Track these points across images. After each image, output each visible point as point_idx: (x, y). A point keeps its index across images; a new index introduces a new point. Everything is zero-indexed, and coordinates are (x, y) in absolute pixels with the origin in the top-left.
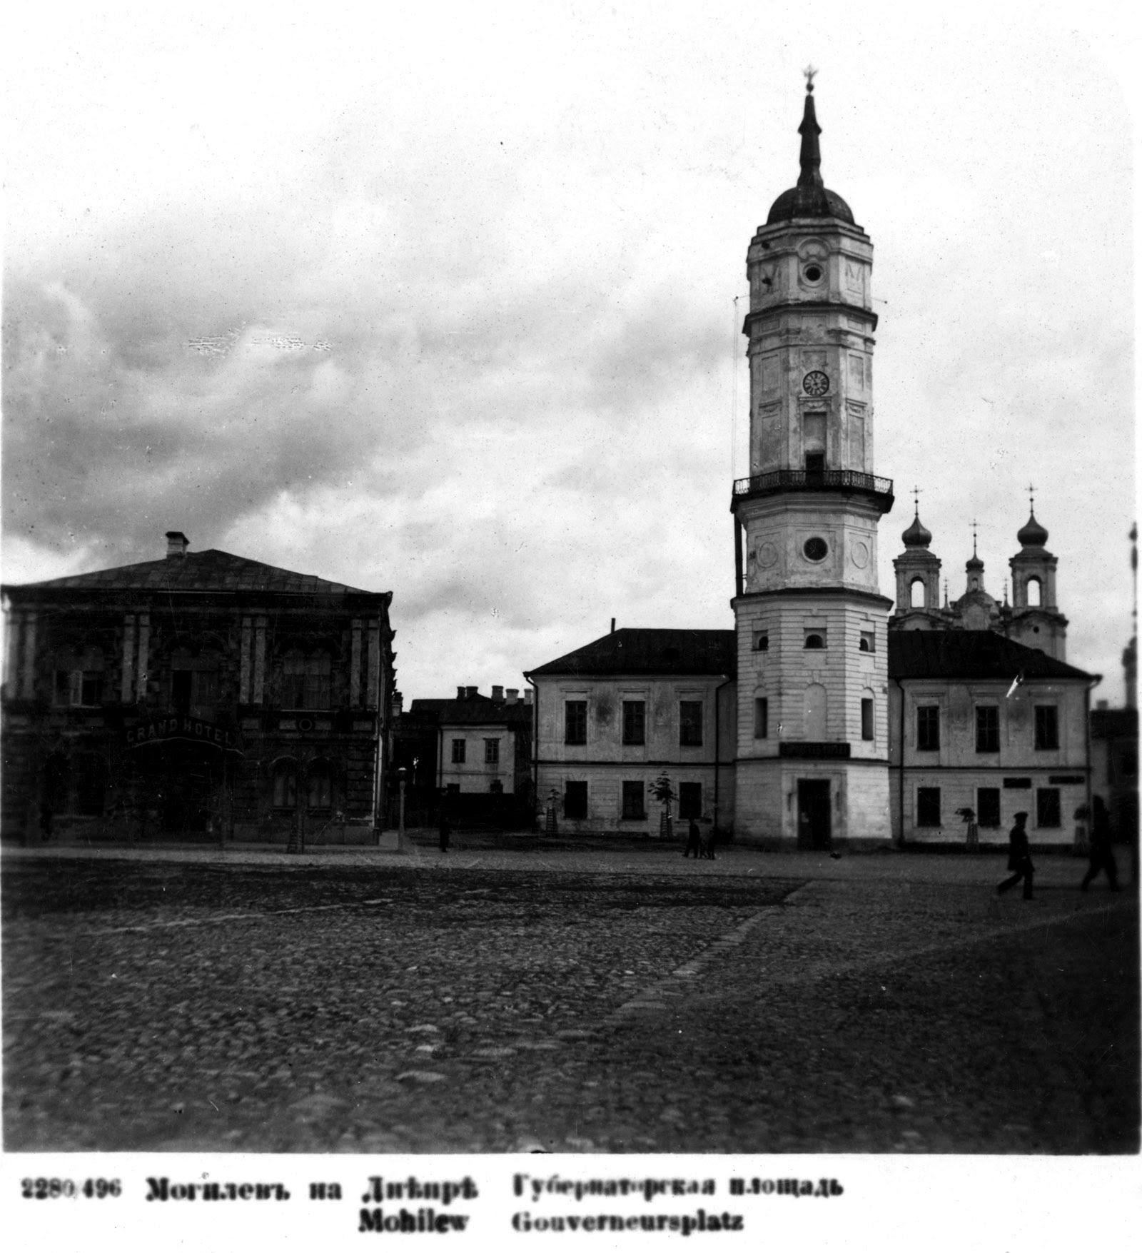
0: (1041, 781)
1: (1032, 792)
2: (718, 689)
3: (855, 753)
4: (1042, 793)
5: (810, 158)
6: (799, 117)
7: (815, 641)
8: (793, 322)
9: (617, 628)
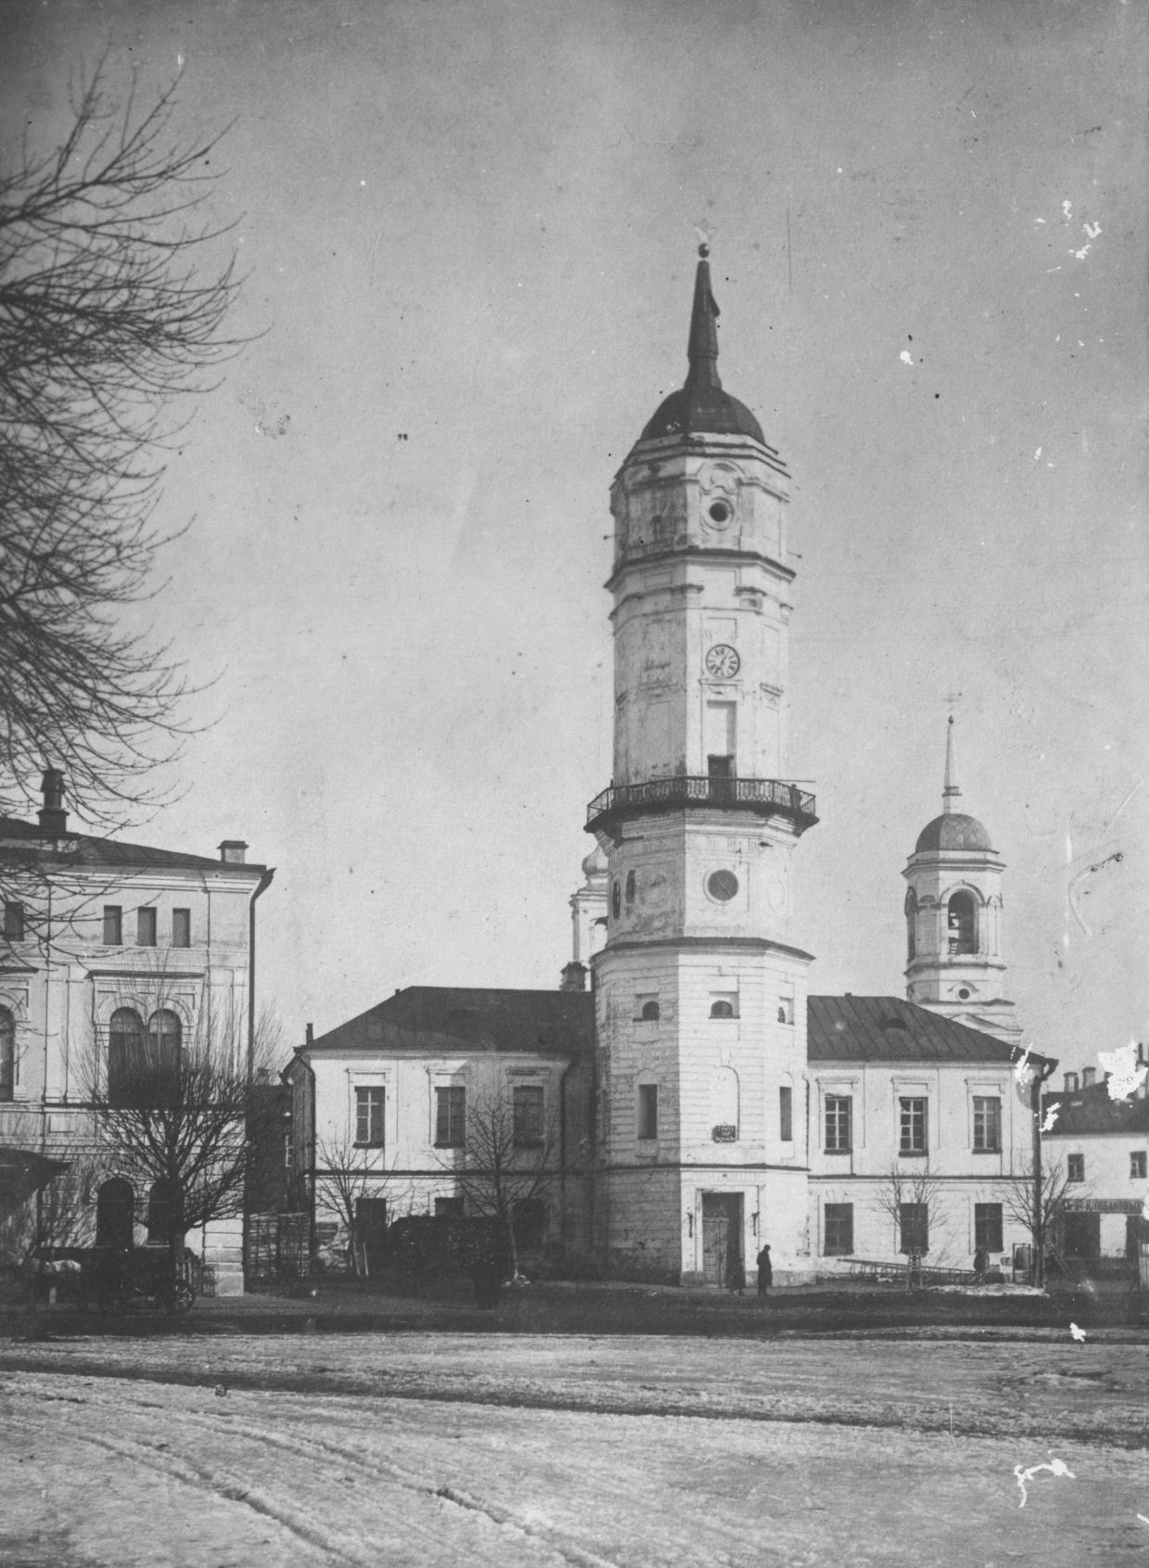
7: (722, 1010)
8: (695, 573)
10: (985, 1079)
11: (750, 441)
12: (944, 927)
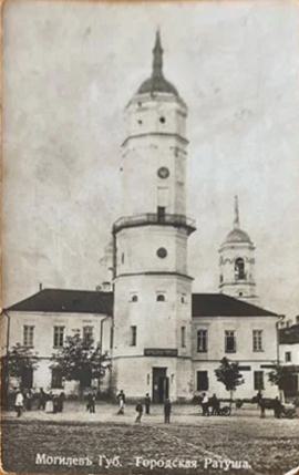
0: (256, 367)
1: (252, 372)
2: (102, 322)
3: (179, 354)
4: (256, 373)
5: (158, 65)
6: (153, 45)
9: (43, 288)
10: (258, 322)
12: (230, 272)
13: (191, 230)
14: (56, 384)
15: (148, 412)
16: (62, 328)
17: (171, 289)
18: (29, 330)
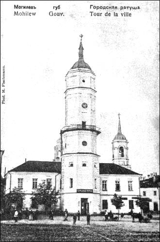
0: (130, 198)
2: (56, 176)
4: (130, 201)
5: (81, 55)
7: (84, 165)
11: (88, 69)
12: (117, 153)
13: (98, 133)
14: (34, 205)
15: (79, 220)
16: (36, 180)
17: (89, 159)
18: (20, 180)
